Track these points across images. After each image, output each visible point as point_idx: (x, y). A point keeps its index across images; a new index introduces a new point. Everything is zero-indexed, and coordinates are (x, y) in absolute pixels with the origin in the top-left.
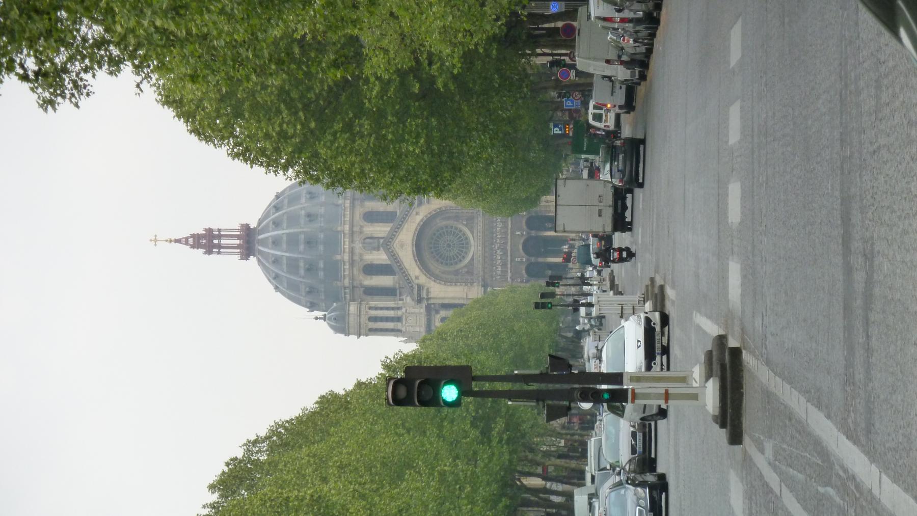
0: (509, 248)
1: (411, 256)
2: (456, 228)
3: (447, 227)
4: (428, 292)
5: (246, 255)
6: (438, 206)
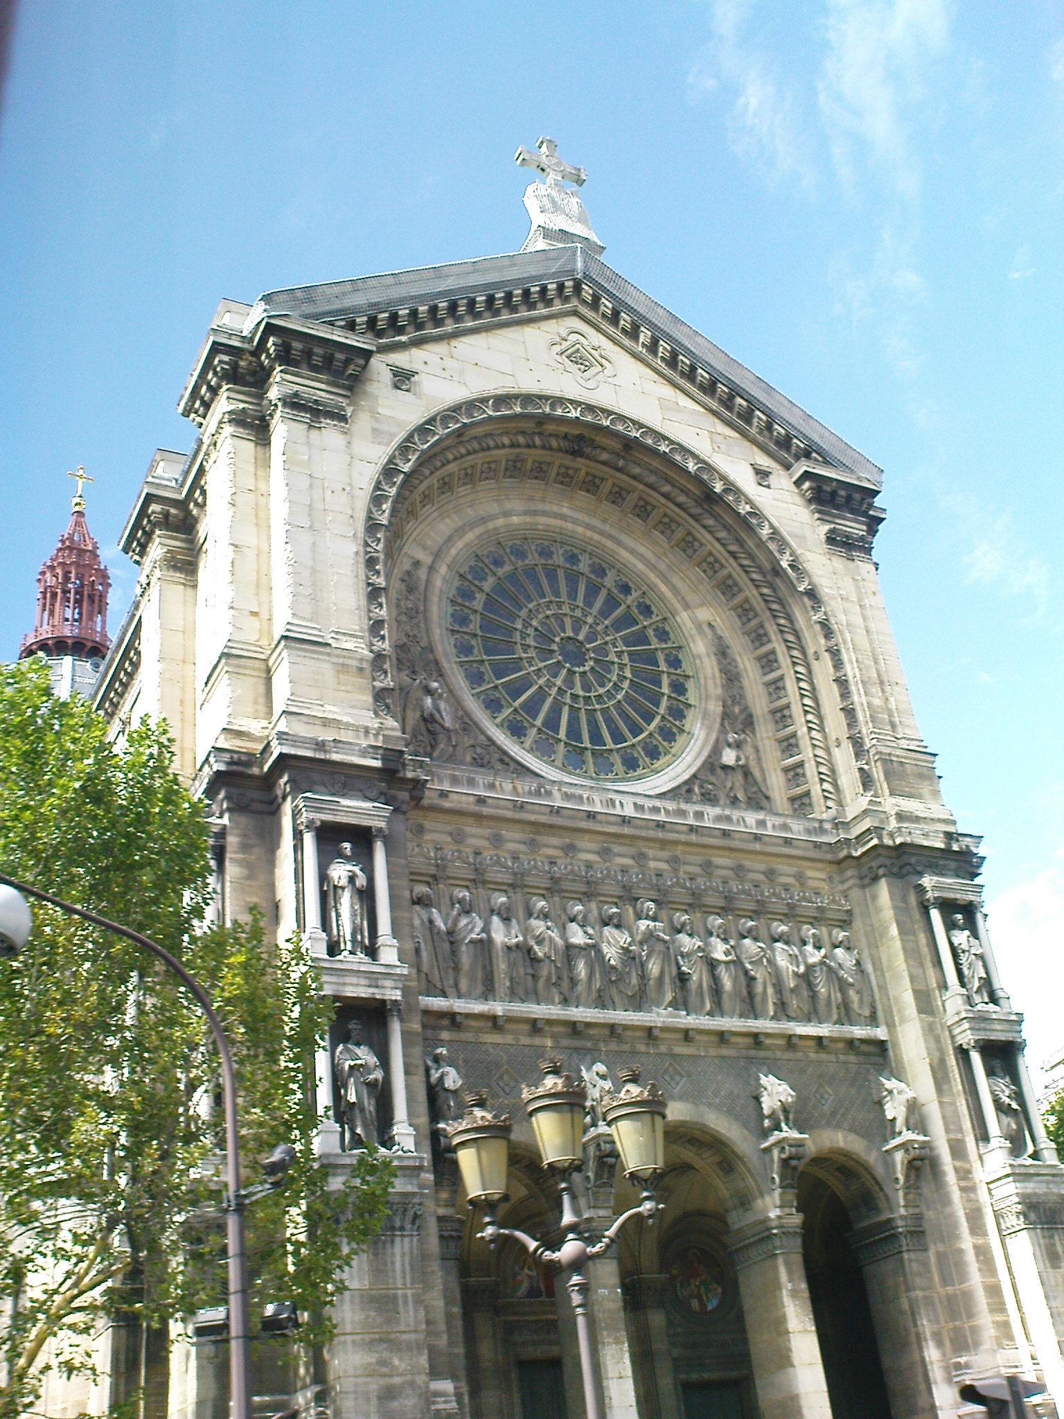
0: (659, 1016)
1: (528, 385)
2: (678, 713)
3: (675, 663)
6: (826, 588)
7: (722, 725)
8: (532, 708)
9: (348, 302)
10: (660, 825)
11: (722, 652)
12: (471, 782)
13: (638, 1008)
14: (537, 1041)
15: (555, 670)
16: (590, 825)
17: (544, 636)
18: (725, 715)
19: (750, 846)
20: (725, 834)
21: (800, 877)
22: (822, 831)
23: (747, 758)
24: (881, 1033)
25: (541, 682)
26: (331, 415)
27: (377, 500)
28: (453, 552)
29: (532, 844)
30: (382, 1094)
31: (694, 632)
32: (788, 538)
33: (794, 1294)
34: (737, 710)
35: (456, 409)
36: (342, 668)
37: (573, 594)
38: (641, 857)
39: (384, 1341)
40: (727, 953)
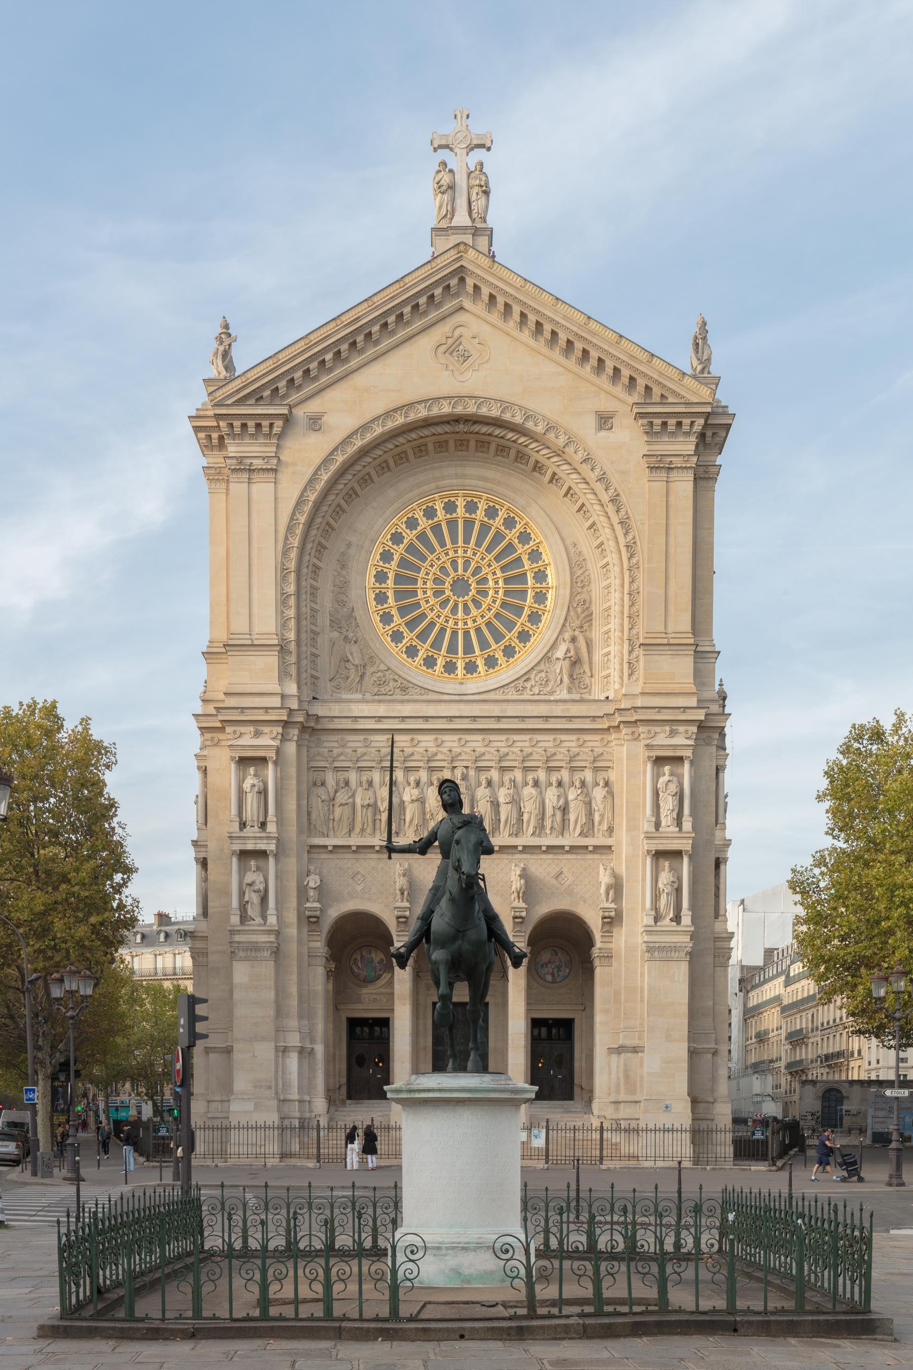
15: (444, 604)
17: (436, 580)
23: (577, 650)
34: (579, 610)
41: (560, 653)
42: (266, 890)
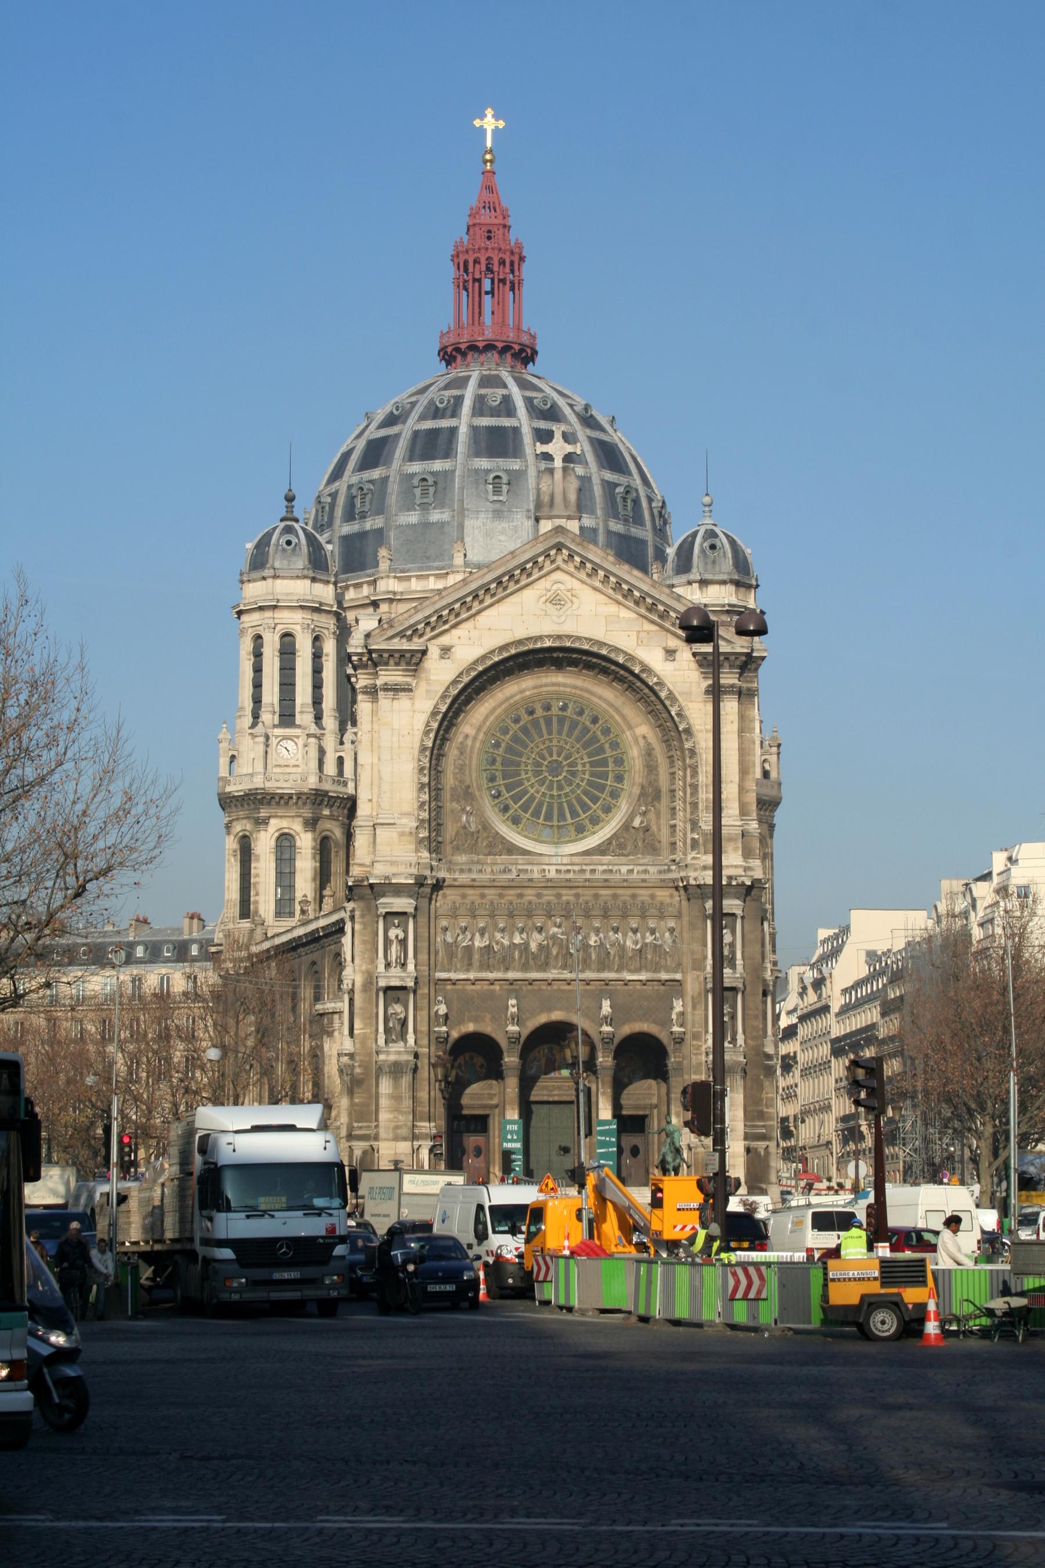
0: (552, 974)
1: (520, 633)
2: (615, 795)
3: (619, 761)
4: (395, 690)
5: (450, 355)
7: (639, 800)
8: (525, 808)
9: (412, 621)
10: (569, 880)
11: (649, 753)
12: (470, 871)
13: (545, 971)
14: (492, 987)
16: (530, 884)
17: (538, 764)
18: (643, 794)
19: (621, 885)
20: (606, 880)
21: (653, 897)
22: (669, 870)
24: (678, 976)
25: (532, 791)
26: (404, 690)
27: (426, 733)
28: (488, 723)
29: (501, 896)
30: (404, 1023)
31: (632, 743)
32: (678, 696)
33: (603, 1094)
35: (476, 662)
36: (402, 834)
37: (560, 733)
38: (559, 896)
39: (396, 1110)
40: (596, 942)
41: (637, 823)
42: (406, 1019)
